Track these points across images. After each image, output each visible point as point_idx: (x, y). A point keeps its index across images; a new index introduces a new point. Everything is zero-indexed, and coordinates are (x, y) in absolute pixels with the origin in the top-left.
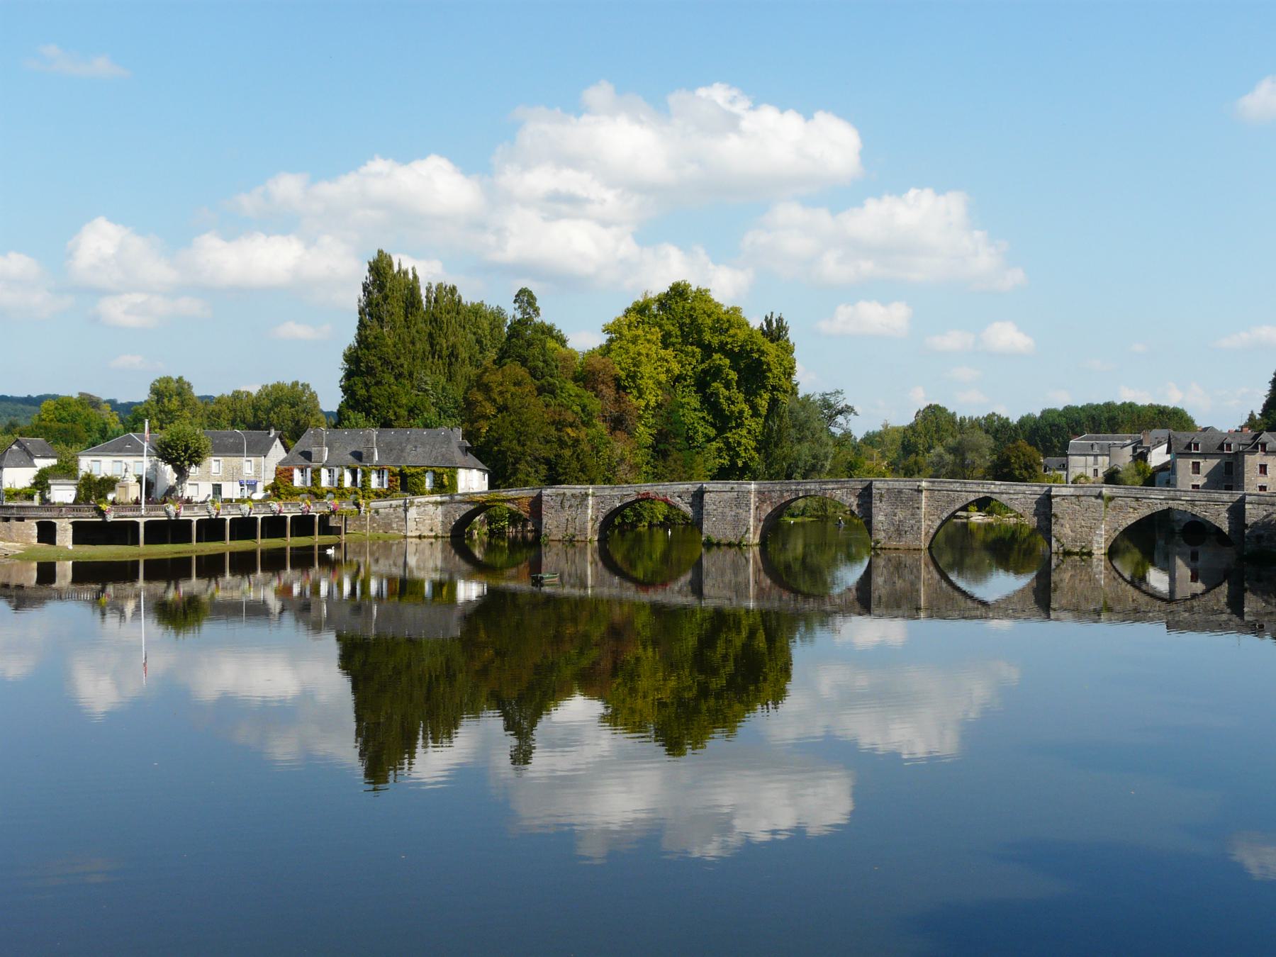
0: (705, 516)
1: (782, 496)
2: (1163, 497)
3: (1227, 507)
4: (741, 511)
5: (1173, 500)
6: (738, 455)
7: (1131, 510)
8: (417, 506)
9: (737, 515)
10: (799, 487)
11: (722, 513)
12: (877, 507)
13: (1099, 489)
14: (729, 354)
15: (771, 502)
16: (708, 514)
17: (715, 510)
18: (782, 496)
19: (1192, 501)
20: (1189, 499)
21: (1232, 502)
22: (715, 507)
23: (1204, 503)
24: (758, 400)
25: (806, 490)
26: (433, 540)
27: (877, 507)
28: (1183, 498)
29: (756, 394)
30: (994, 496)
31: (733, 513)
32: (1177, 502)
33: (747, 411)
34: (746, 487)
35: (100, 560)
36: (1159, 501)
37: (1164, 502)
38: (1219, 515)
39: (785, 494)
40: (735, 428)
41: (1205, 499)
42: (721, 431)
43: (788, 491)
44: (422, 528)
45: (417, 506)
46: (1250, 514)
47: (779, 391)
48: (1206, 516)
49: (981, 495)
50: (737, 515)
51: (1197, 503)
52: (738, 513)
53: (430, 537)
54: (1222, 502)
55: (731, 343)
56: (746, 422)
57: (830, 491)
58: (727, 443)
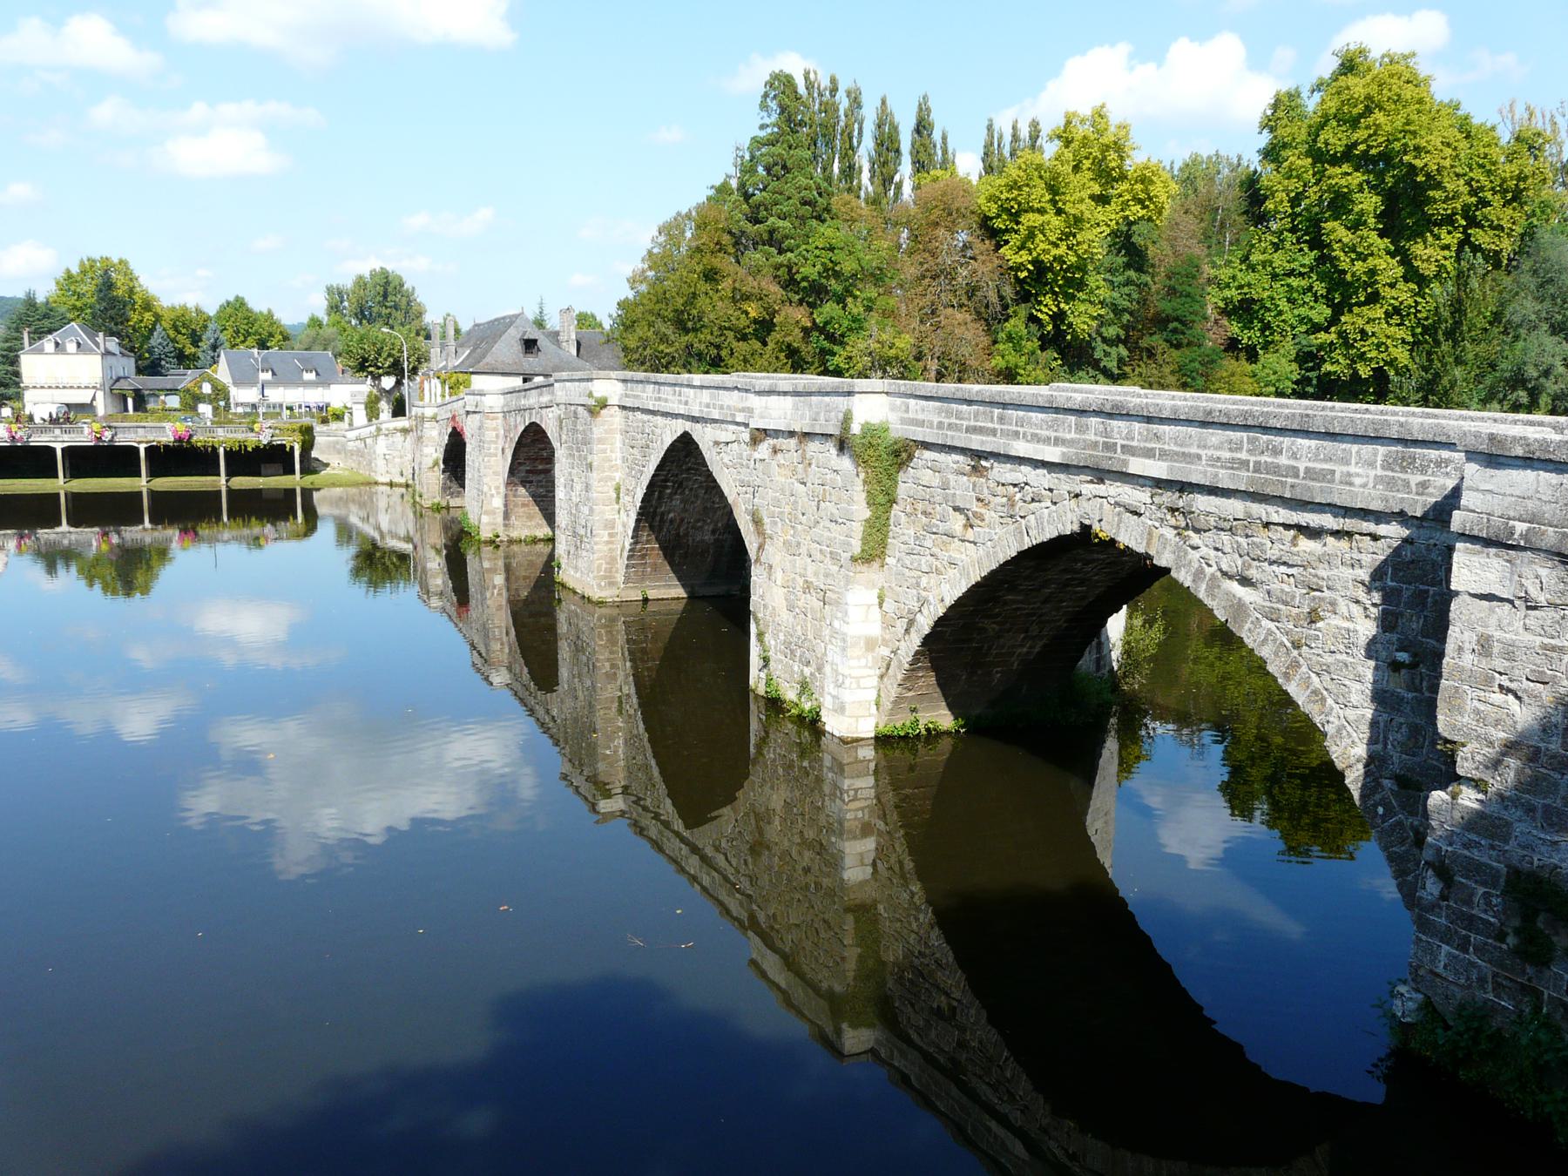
2: (1053, 454)
3: (1373, 555)
5: (1100, 474)
6: (1362, 356)
7: (957, 523)
8: (386, 435)
13: (841, 402)
14: (1364, 162)
19: (1184, 487)
20: (1158, 469)
21: (1401, 517)
23: (1235, 507)
24: (1418, 249)
26: (403, 490)
28: (1137, 466)
29: (1417, 234)
32: (1113, 489)
33: (1390, 268)
35: (125, 490)
36: (1040, 478)
37: (1064, 483)
38: (1313, 617)
40: (1359, 304)
41: (1241, 481)
42: (1338, 310)
44: (393, 470)
45: (386, 435)
46: (1484, 646)
47: (1482, 227)
48: (1239, 608)
51: (1202, 502)
53: (400, 485)
54: (1347, 512)
55: (1365, 141)
56: (1387, 292)
58: (1342, 335)
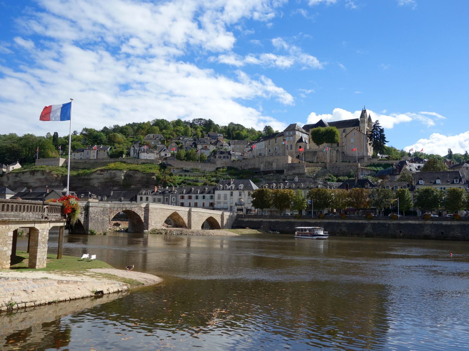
0: (90, 220)
1: (117, 210)
4: (105, 217)
9: (103, 219)
10: (124, 206)
11: (97, 218)
12: (150, 215)
15: (114, 213)
16: (91, 219)
17: (94, 216)
18: (117, 210)
22: (94, 215)
25: (126, 208)
27: (150, 215)
30: (177, 212)
31: (102, 218)
34: (107, 206)
39: (119, 209)
43: (120, 208)
49: (174, 211)
50: (103, 219)
52: (104, 218)
57: (133, 208)
